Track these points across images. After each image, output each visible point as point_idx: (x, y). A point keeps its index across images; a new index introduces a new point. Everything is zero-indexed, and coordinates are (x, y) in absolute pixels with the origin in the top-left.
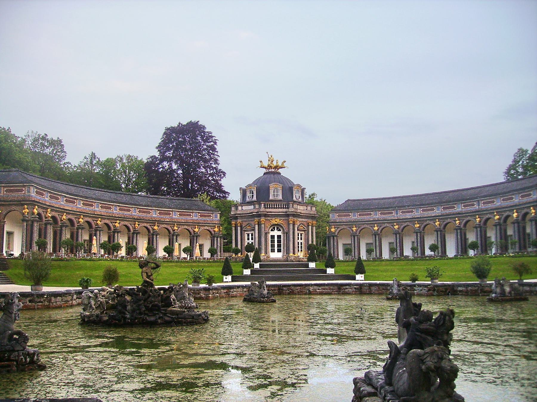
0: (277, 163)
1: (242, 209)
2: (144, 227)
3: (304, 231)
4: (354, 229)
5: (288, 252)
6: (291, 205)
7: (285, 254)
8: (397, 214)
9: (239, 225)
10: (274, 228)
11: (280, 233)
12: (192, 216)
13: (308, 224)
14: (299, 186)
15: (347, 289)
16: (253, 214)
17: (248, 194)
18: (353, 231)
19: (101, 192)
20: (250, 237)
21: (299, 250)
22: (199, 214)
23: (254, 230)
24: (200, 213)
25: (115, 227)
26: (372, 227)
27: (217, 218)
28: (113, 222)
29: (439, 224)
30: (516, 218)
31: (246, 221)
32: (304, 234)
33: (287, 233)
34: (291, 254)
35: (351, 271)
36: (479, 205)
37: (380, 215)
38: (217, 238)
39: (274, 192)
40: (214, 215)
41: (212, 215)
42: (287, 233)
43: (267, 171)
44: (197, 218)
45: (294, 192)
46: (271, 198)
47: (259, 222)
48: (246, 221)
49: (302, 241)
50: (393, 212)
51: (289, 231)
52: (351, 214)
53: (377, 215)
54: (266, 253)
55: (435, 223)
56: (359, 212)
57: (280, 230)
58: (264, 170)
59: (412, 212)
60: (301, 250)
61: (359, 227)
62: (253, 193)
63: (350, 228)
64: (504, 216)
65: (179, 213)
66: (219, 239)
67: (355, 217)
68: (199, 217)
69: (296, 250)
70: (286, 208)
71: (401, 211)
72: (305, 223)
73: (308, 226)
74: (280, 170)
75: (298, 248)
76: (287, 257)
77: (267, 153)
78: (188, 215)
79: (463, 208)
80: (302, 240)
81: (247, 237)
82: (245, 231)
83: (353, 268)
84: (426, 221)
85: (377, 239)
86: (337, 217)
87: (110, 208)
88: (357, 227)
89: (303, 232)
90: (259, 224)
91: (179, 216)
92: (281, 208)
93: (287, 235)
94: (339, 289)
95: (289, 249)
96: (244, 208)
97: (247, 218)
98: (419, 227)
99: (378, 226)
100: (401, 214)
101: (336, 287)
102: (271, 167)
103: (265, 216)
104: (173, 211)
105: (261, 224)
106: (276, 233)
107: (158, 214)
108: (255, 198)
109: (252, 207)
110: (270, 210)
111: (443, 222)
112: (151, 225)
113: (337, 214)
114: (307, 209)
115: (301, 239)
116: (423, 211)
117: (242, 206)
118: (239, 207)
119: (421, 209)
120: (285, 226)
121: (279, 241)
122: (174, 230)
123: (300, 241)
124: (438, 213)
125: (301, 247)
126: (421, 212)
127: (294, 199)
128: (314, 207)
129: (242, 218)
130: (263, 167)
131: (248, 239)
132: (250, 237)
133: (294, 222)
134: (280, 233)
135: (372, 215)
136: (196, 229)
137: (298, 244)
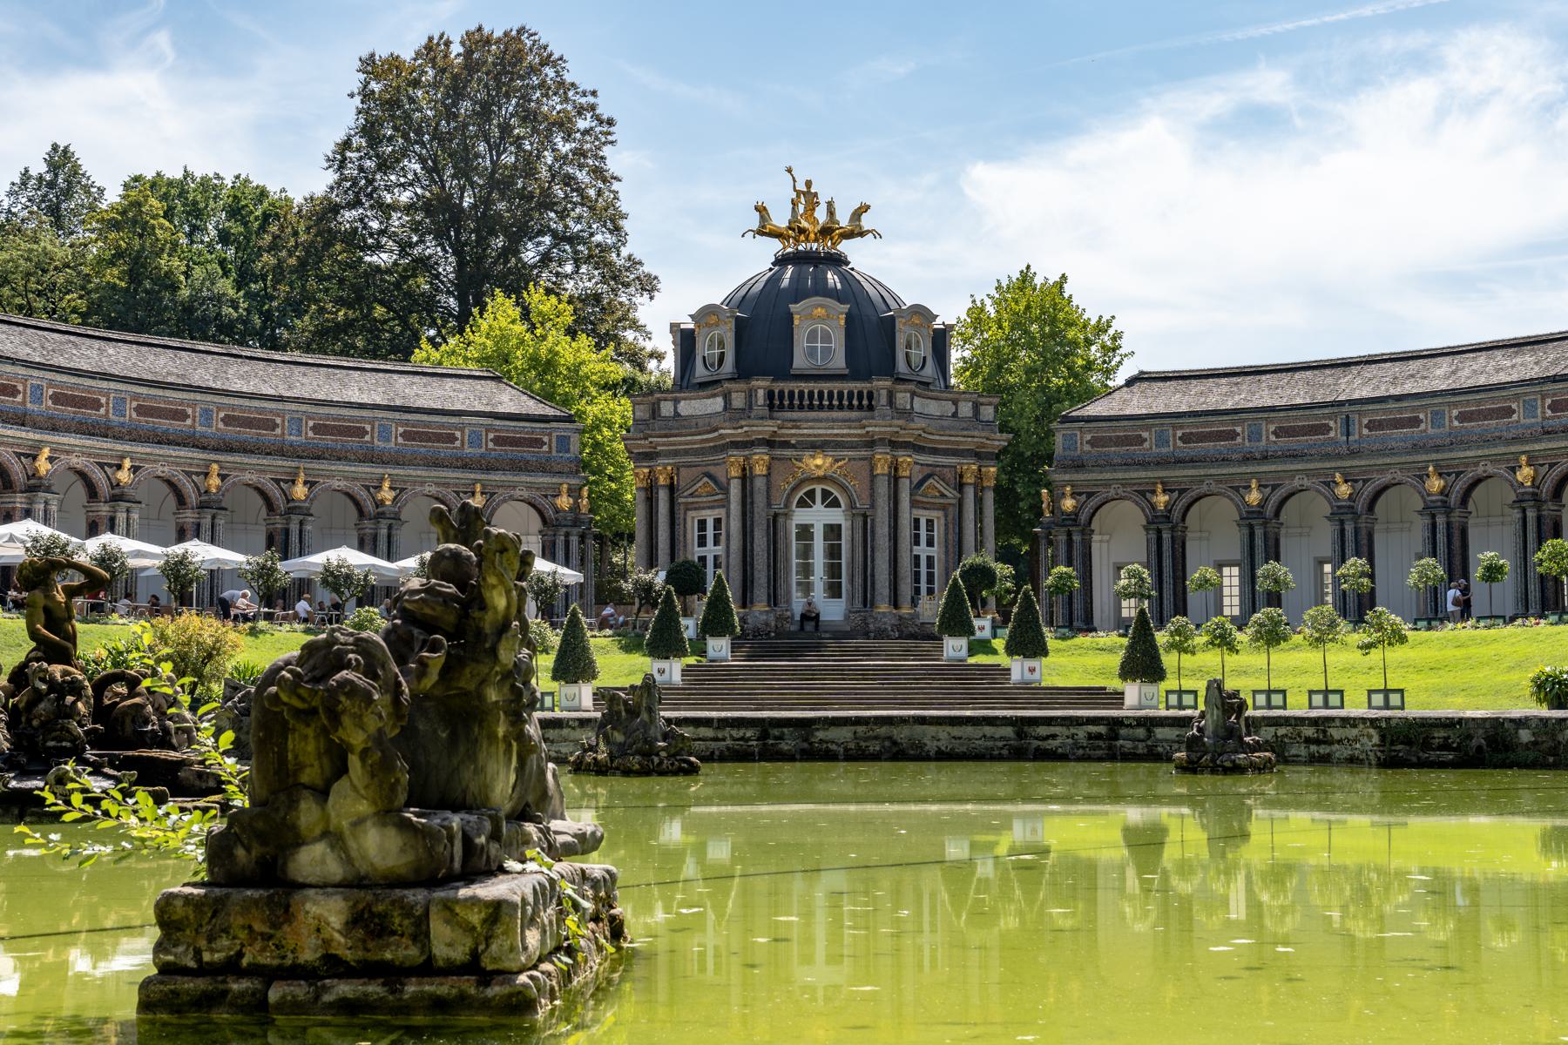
0: (831, 212)
1: (677, 414)
2: (258, 489)
3: (944, 508)
4: (1161, 499)
5: (868, 601)
6: (884, 393)
7: (858, 604)
8: (1348, 435)
9: (662, 480)
10: (811, 494)
11: (837, 516)
12: (458, 443)
13: (961, 476)
14: (922, 314)
15: (1054, 736)
16: (722, 431)
17: (703, 349)
18: (1153, 507)
19: (56, 336)
20: (710, 532)
21: (917, 591)
22: (491, 436)
23: (725, 504)
24: (497, 431)
25: (118, 485)
26: (1236, 489)
27: (568, 451)
28: (110, 466)
29: (1534, 479)
31: (690, 466)
32: (943, 521)
33: (865, 516)
34: (884, 607)
35: (1102, 672)
37: (1273, 438)
38: (567, 535)
39: (812, 337)
40: (554, 440)
41: (546, 439)
42: (865, 516)
43: (789, 250)
44: (483, 450)
45: (900, 340)
46: (800, 362)
47: (744, 469)
48: (690, 466)
49: (934, 551)
50: (1332, 424)
51: (873, 506)
52: (1145, 435)
53: (1259, 440)
54: (773, 599)
55: (1513, 470)
56: (1181, 427)
57: (835, 504)
58: (774, 247)
59: (1415, 422)
60: (930, 591)
61: (1182, 491)
62: (721, 344)
63: (1142, 493)
65: (401, 430)
66: (574, 540)
67: (1164, 450)
68: (491, 445)
69: (906, 589)
70: (860, 407)
71: (1365, 421)
72: (949, 475)
73: (960, 487)
74: (846, 247)
75: (917, 579)
76: (864, 620)
77: (789, 171)
78: (439, 438)
80: (936, 548)
81: (696, 533)
82: (689, 507)
83: (1116, 660)
84: (1476, 464)
85: (1259, 542)
86: (1087, 448)
88: (1172, 491)
89: (934, 514)
90: (746, 478)
91: (400, 440)
92: (841, 407)
93: (865, 523)
94: (1020, 735)
95: (873, 583)
96: (686, 408)
97: (696, 452)
98: (1443, 492)
99: (1265, 486)
100: (1365, 431)
101: (1008, 731)
102: (802, 231)
103: (770, 444)
104: (372, 421)
105: (752, 477)
106: (818, 517)
107: (310, 434)
108: (729, 365)
109: (717, 404)
110: (796, 415)
111: (1551, 466)
112: (277, 481)
113: (1088, 437)
114: (955, 415)
115: (930, 543)
116: (1463, 417)
117: (676, 401)
118: (663, 404)
119: (1455, 412)
120: (857, 485)
121: (833, 552)
122: (379, 504)
123: (923, 550)
124: (1528, 427)
125: (930, 577)
126: (1456, 423)
127: (901, 366)
128: (990, 404)
129: (676, 453)
130: (776, 234)
131: (702, 542)
132: (710, 532)
133: (896, 469)
134: (837, 516)
135: (1239, 440)
136: (478, 496)
137: (917, 565)
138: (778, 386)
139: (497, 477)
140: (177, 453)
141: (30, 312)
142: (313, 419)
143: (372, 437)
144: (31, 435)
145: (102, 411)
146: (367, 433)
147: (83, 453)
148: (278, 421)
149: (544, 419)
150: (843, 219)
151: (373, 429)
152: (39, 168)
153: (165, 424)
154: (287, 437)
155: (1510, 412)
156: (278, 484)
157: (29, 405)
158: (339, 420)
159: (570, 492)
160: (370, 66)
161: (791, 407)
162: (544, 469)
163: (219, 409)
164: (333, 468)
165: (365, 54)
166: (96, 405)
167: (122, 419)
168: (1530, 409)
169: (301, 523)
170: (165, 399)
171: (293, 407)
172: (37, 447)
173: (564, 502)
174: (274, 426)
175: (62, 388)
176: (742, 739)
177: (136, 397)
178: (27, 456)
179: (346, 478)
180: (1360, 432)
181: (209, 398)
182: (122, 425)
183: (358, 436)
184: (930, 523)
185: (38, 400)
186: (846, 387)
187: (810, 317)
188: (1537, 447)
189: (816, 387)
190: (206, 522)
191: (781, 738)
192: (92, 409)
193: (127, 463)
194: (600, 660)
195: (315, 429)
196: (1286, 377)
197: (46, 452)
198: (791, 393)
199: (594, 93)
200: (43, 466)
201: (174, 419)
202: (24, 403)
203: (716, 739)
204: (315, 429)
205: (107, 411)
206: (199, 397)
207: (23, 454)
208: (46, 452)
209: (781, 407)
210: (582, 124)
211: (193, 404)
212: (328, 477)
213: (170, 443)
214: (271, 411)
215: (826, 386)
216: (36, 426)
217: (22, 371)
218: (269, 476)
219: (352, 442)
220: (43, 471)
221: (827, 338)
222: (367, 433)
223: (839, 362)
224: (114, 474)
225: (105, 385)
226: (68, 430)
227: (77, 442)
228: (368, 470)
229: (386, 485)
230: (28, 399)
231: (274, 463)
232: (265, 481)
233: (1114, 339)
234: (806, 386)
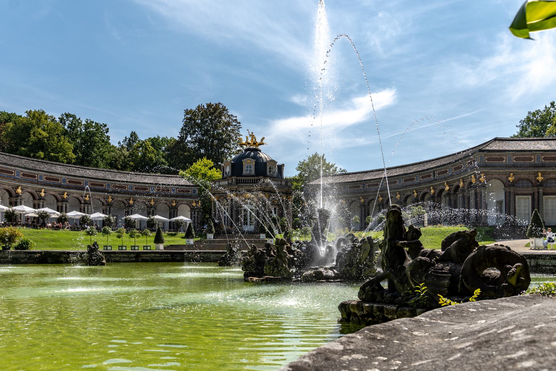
8: (364, 188)
30: (462, 187)
36: (434, 176)
39: (247, 167)
46: (244, 173)
55: (396, 195)
64: (454, 186)
74: (260, 147)
79: (421, 179)
98: (382, 201)
108: (230, 174)
110: (242, 185)
112: (126, 200)
114: (281, 184)
117: (219, 182)
122: (151, 205)
127: (268, 173)
138: (238, 178)
139: (178, 199)
141: (63, 162)
144: (62, 190)
145: (82, 184)
149: (189, 186)
150: (258, 141)
152: (129, 136)
153: (98, 187)
155: (396, 182)
159: (196, 202)
160: (187, 112)
161: (241, 183)
162: (190, 197)
163: (112, 184)
165: (185, 109)
166: (80, 183)
168: (400, 182)
172: (64, 192)
173: (194, 204)
176: (167, 257)
177: (90, 181)
178: (62, 194)
180: (367, 187)
181: (109, 182)
184: (275, 209)
185: (65, 182)
186: (254, 178)
187: (246, 163)
188: (401, 190)
189: (249, 178)
190: (86, 208)
191: (177, 256)
194: (165, 239)
195: (135, 188)
196: (354, 175)
197: (66, 193)
198: (242, 180)
199: (236, 117)
200: (65, 196)
203: (160, 257)
204: (135, 188)
206: (106, 181)
208: (66, 193)
209: (239, 183)
210: (234, 124)
211: (105, 183)
215: (251, 178)
217: (60, 176)
221: (250, 167)
223: (253, 172)
225: (82, 179)
226: (72, 189)
229: (152, 201)
232: (124, 200)
233: (335, 168)
234: (247, 178)
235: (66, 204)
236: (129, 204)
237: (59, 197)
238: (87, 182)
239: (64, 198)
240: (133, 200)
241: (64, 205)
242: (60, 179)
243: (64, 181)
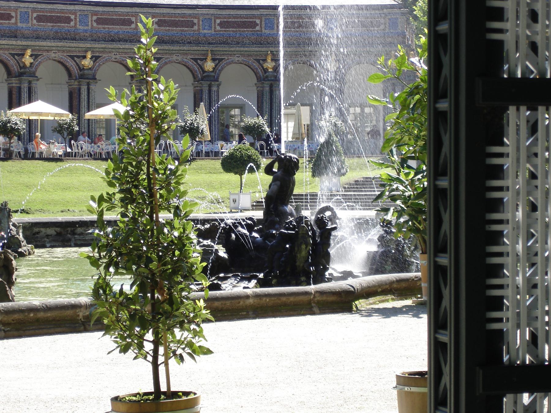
28: (78, 57)
87: (68, 20)
104: (260, 17)
107: (218, 28)
112: (195, 60)
122: (265, 71)
140: (123, 46)
142: (220, 18)
143: (261, 27)
144: (19, 43)
145: (72, 24)
146: (257, 25)
147: (59, 51)
148: (196, 21)
151: (261, 22)
153: (116, 29)
154: (201, 31)
156: (197, 62)
157: (19, 25)
158: (237, 18)
164: (232, 49)
166: (68, 20)
167: (86, 28)
169: (210, 86)
170: (116, 13)
171: (204, 11)
174: (194, 24)
175: (43, 12)
177: (95, 13)
179: (243, 55)
182: (86, 31)
183: (251, 27)
185: (27, 21)
192: (65, 23)
193: (89, 55)
195: (221, 24)
197: (29, 52)
200: (28, 60)
201: (122, 25)
202: (16, 23)
204: (221, 24)
205: (76, 24)
207: (17, 54)
208: (29, 52)
212: (231, 55)
213: (120, 40)
214: (190, 15)
216: (25, 37)
218: (189, 57)
219: (247, 31)
220: (28, 64)
222: (257, 25)
224: (81, 62)
226: (46, 38)
227: (53, 44)
228: (257, 49)
230: (19, 21)
231: (192, 48)
232: (188, 59)
235: (30, 83)
236: (204, 72)
237: (12, 62)
238: (86, 16)
239: (25, 66)
240: (213, 60)
241: (25, 86)
242: (13, 14)
243: (25, 17)
